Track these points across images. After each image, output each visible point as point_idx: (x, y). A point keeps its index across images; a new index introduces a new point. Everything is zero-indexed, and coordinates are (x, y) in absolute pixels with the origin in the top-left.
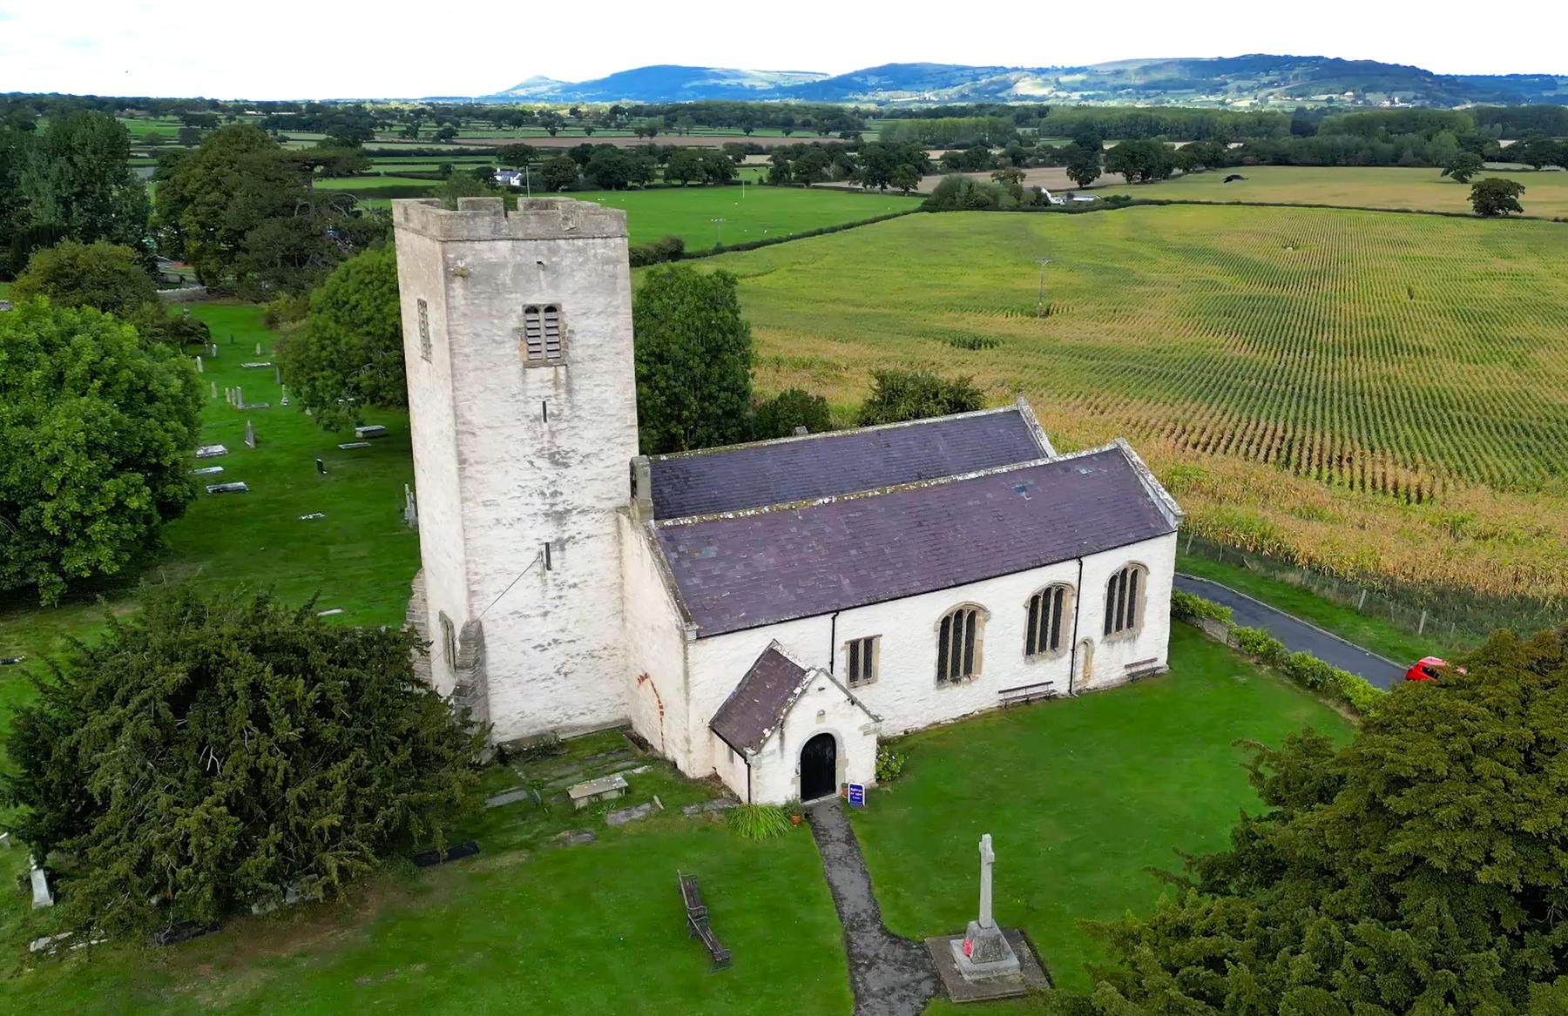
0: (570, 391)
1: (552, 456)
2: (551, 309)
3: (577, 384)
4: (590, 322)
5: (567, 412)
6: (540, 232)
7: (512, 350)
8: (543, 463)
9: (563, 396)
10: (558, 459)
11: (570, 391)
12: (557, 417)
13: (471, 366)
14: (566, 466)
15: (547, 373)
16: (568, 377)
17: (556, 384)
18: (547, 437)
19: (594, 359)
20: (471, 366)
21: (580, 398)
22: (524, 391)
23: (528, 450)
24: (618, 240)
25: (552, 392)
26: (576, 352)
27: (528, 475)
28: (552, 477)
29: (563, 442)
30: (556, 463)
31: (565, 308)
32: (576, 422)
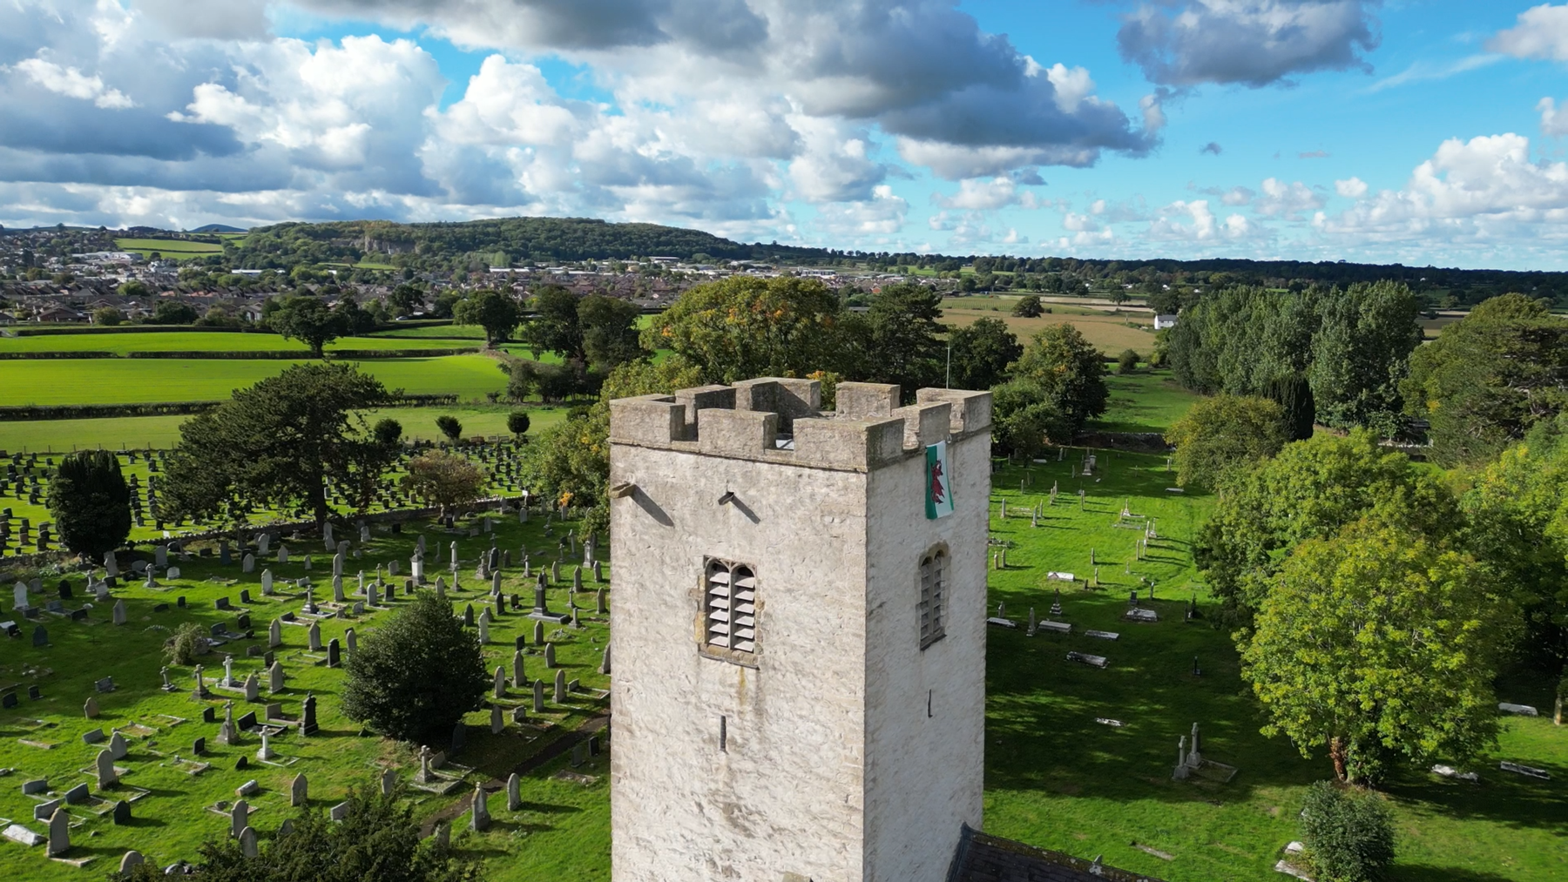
0: (759, 712)
1: (729, 809)
2: (744, 571)
3: (771, 704)
4: (796, 606)
5: (754, 745)
6: (734, 445)
7: (683, 623)
8: (717, 816)
9: (750, 716)
10: (734, 814)
11: (759, 712)
12: (740, 748)
13: (634, 630)
14: (750, 836)
15: (731, 671)
16: (759, 688)
17: (741, 695)
18: (722, 776)
19: (799, 671)
20: (634, 630)
21: (774, 729)
22: (695, 692)
23: (697, 785)
24: (853, 478)
25: (735, 705)
26: (774, 651)
27: (694, 824)
28: (727, 843)
29: (746, 791)
30: (734, 823)
31: (761, 572)
32: (765, 768)
